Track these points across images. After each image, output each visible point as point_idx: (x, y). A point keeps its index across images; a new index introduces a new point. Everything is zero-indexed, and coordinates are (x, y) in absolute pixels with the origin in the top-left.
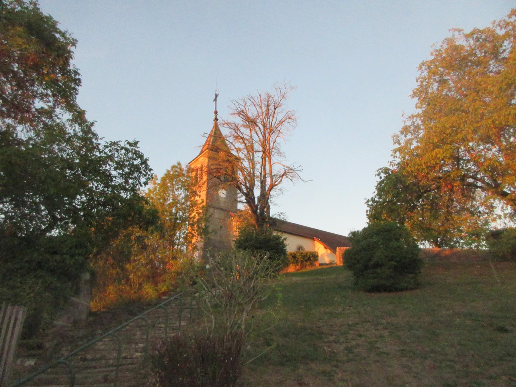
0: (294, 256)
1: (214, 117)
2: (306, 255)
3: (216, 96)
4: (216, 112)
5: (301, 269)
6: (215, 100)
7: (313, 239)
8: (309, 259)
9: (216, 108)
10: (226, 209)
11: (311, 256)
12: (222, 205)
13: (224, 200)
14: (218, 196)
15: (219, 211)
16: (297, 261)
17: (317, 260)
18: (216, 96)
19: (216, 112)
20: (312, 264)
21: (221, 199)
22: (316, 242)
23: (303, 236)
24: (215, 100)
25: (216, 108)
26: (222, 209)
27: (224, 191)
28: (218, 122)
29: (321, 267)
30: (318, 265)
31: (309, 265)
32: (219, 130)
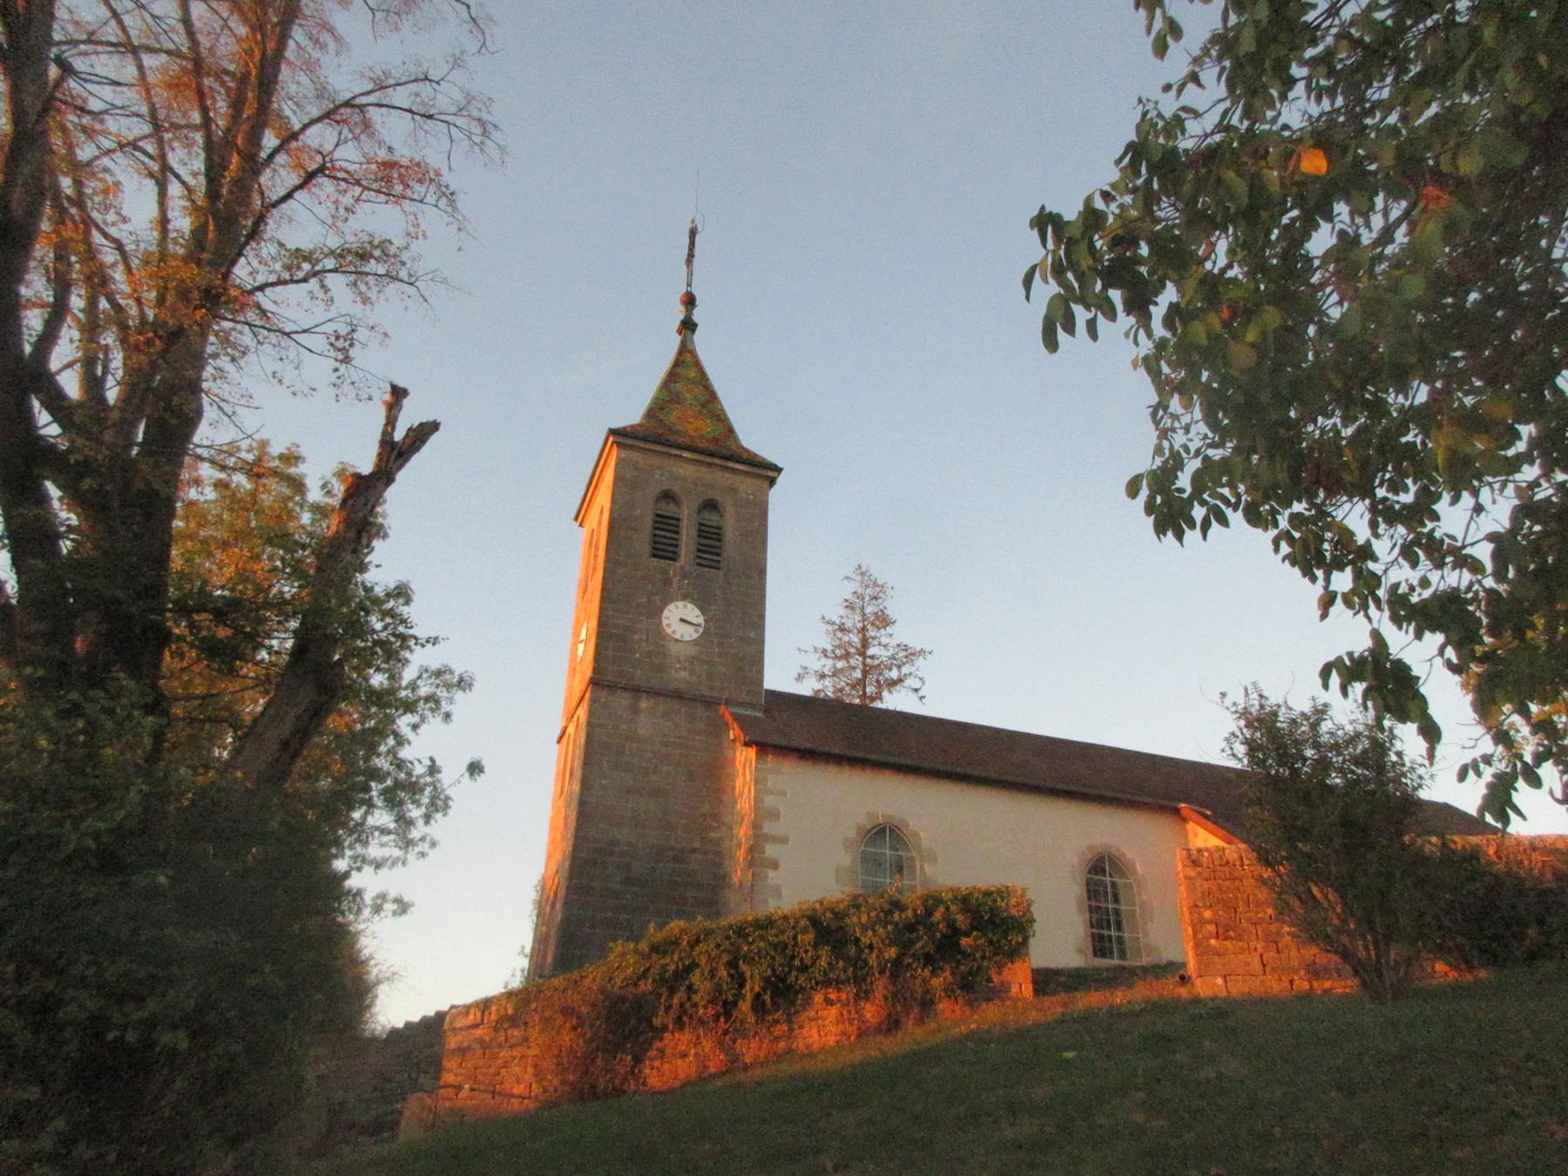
0: (828, 928)
2: (923, 920)
4: (690, 301)
5: (892, 1025)
7: (1176, 812)
8: (947, 948)
9: (689, 285)
11: (962, 921)
12: (679, 676)
13: (692, 651)
14: (659, 634)
16: (859, 963)
17: (1017, 951)
19: (690, 301)
20: (971, 986)
21: (674, 649)
22: (1191, 826)
23: (1070, 795)
25: (689, 285)
26: (678, 696)
27: (692, 612)
29: (1054, 1006)
30: (1028, 990)
31: (949, 992)
32: (697, 364)
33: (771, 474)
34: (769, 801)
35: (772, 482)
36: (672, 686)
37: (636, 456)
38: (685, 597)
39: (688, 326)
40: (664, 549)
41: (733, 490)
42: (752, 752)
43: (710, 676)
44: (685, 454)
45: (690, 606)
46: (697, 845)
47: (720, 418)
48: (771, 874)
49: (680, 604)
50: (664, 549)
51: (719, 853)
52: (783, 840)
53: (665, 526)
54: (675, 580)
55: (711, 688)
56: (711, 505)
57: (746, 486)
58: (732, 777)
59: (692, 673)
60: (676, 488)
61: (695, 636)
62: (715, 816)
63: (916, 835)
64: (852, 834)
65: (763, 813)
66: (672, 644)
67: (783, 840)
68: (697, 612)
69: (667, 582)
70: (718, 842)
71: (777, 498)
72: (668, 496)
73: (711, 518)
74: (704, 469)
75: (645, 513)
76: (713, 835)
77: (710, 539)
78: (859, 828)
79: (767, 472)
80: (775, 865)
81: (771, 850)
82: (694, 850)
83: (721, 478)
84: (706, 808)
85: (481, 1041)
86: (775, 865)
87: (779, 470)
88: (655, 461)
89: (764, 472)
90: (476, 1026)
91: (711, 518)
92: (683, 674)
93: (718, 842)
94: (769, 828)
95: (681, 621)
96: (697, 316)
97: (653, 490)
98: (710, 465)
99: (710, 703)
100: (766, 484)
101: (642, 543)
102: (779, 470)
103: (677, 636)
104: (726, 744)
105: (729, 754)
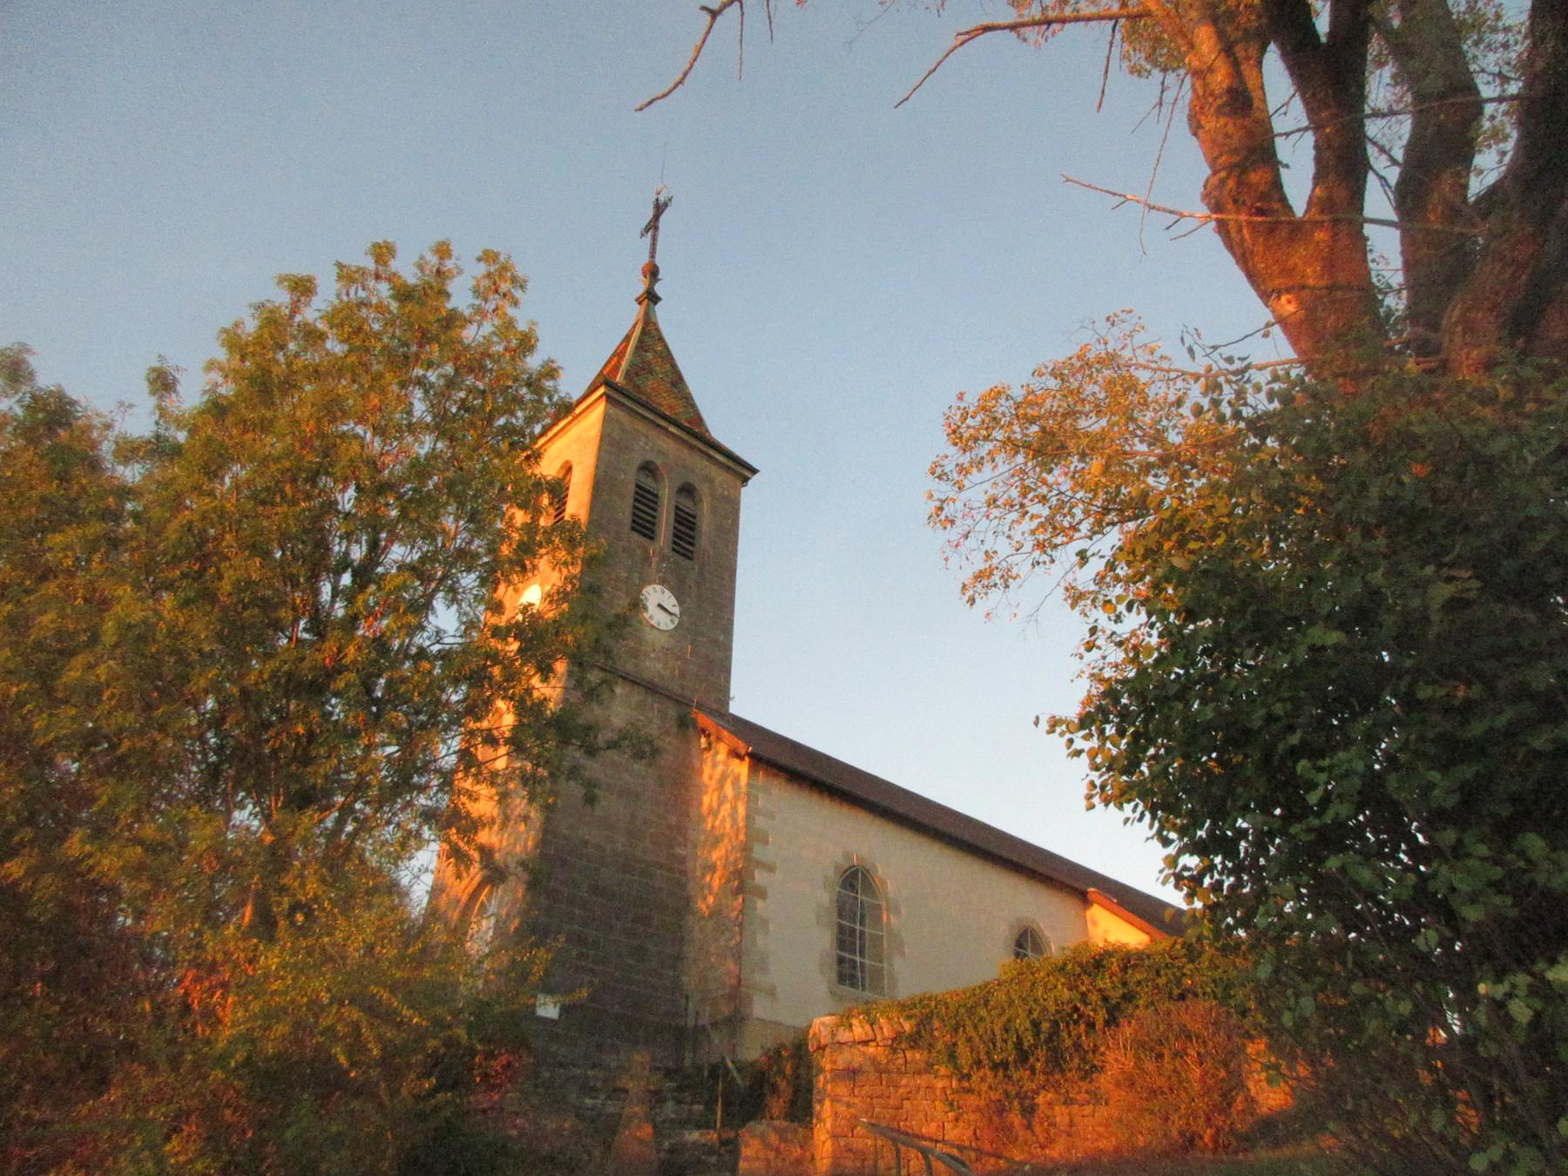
1: (640, 287)
3: (659, 208)
4: (652, 273)
6: (653, 226)
9: (653, 256)
10: (675, 687)
12: (653, 667)
13: (664, 641)
15: (637, 696)
18: (659, 208)
19: (652, 273)
21: (649, 636)
24: (653, 226)
25: (653, 256)
26: (651, 688)
28: (658, 308)
33: (747, 473)
34: (760, 822)
35: (745, 480)
36: (647, 676)
37: (623, 417)
38: (663, 582)
39: (651, 297)
40: (644, 526)
41: (711, 481)
42: (742, 769)
43: (682, 675)
44: (672, 429)
45: (667, 593)
46: (662, 860)
47: (687, 399)
48: (760, 904)
49: (658, 587)
50: (644, 526)
51: (683, 873)
52: (771, 868)
53: (645, 500)
54: (655, 560)
55: (682, 687)
56: (687, 490)
57: (721, 477)
58: (701, 789)
59: (666, 663)
60: (659, 462)
61: (671, 626)
62: (681, 829)
63: (884, 883)
64: (831, 873)
65: (753, 837)
66: (648, 629)
67: (771, 868)
68: (673, 601)
69: (647, 559)
70: (683, 860)
71: (750, 496)
72: (648, 468)
73: (686, 504)
74: (685, 453)
75: (629, 477)
76: (679, 851)
77: (686, 526)
78: (837, 867)
79: (742, 471)
80: (762, 894)
81: (760, 877)
82: (661, 867)
83: (701, 464)
84: (673, 820)
85: (874, 1060)
86: (762, 894)
87: (754, 471)
88: (641, 427)
89: (739, 469)
90: (865, 1043)
91: (686, 504)
92: (659, 666)
93: (683, 860)
94: (758, 852)
95: (660, 606)
96: (659, 289)
97: (638, 460)
98: (692, 447)
99: (681, 702)
100: (739, 483)
101: (624, 510)
102: (754, 471)
103: (654, 622)
104: (694, 751)
105: (696, 763)
